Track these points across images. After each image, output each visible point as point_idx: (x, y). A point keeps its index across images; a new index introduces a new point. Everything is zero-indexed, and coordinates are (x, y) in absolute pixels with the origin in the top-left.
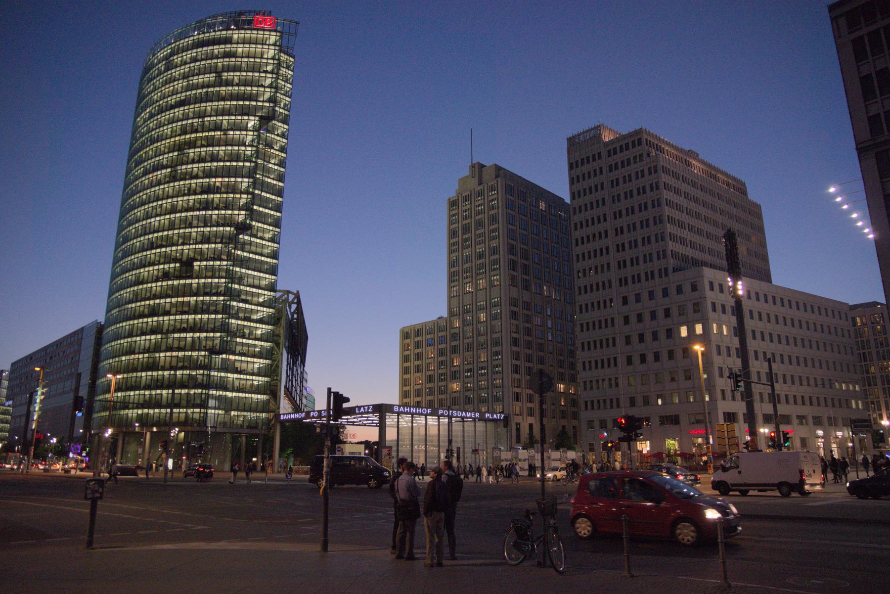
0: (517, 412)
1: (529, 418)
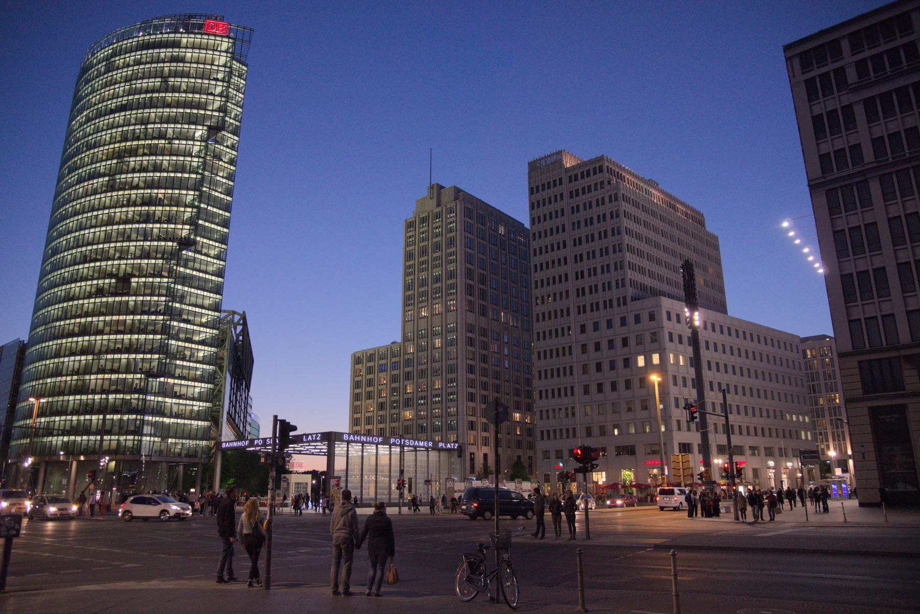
0: (472, 442)
1: (483, 448)
